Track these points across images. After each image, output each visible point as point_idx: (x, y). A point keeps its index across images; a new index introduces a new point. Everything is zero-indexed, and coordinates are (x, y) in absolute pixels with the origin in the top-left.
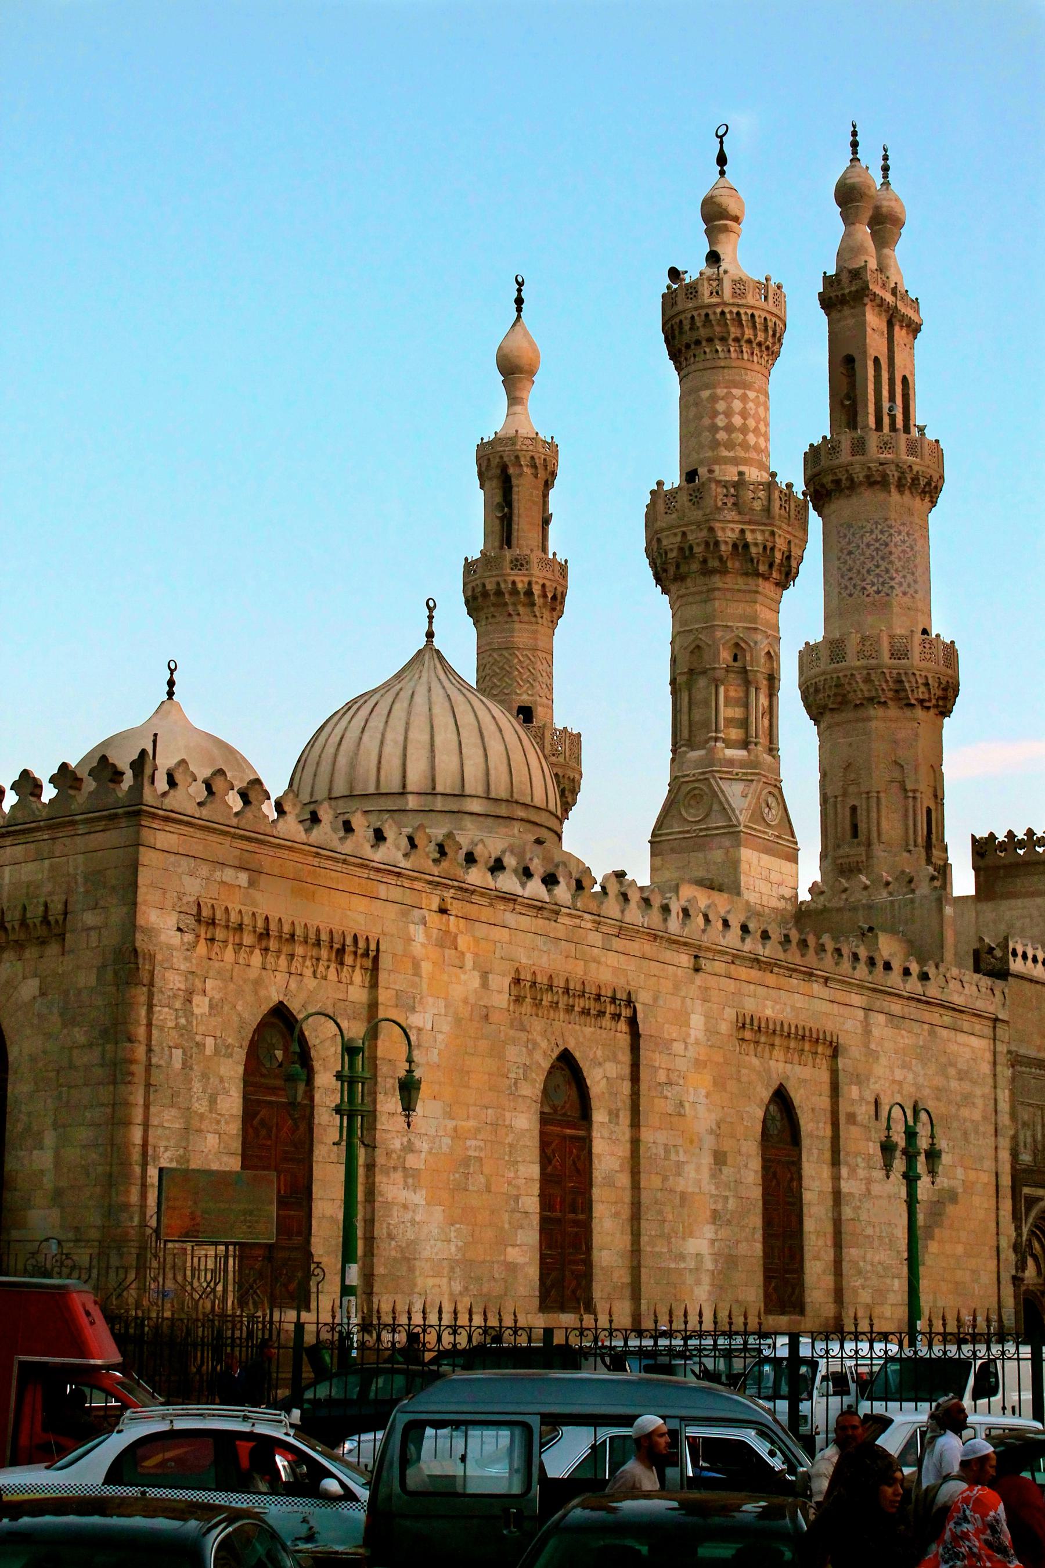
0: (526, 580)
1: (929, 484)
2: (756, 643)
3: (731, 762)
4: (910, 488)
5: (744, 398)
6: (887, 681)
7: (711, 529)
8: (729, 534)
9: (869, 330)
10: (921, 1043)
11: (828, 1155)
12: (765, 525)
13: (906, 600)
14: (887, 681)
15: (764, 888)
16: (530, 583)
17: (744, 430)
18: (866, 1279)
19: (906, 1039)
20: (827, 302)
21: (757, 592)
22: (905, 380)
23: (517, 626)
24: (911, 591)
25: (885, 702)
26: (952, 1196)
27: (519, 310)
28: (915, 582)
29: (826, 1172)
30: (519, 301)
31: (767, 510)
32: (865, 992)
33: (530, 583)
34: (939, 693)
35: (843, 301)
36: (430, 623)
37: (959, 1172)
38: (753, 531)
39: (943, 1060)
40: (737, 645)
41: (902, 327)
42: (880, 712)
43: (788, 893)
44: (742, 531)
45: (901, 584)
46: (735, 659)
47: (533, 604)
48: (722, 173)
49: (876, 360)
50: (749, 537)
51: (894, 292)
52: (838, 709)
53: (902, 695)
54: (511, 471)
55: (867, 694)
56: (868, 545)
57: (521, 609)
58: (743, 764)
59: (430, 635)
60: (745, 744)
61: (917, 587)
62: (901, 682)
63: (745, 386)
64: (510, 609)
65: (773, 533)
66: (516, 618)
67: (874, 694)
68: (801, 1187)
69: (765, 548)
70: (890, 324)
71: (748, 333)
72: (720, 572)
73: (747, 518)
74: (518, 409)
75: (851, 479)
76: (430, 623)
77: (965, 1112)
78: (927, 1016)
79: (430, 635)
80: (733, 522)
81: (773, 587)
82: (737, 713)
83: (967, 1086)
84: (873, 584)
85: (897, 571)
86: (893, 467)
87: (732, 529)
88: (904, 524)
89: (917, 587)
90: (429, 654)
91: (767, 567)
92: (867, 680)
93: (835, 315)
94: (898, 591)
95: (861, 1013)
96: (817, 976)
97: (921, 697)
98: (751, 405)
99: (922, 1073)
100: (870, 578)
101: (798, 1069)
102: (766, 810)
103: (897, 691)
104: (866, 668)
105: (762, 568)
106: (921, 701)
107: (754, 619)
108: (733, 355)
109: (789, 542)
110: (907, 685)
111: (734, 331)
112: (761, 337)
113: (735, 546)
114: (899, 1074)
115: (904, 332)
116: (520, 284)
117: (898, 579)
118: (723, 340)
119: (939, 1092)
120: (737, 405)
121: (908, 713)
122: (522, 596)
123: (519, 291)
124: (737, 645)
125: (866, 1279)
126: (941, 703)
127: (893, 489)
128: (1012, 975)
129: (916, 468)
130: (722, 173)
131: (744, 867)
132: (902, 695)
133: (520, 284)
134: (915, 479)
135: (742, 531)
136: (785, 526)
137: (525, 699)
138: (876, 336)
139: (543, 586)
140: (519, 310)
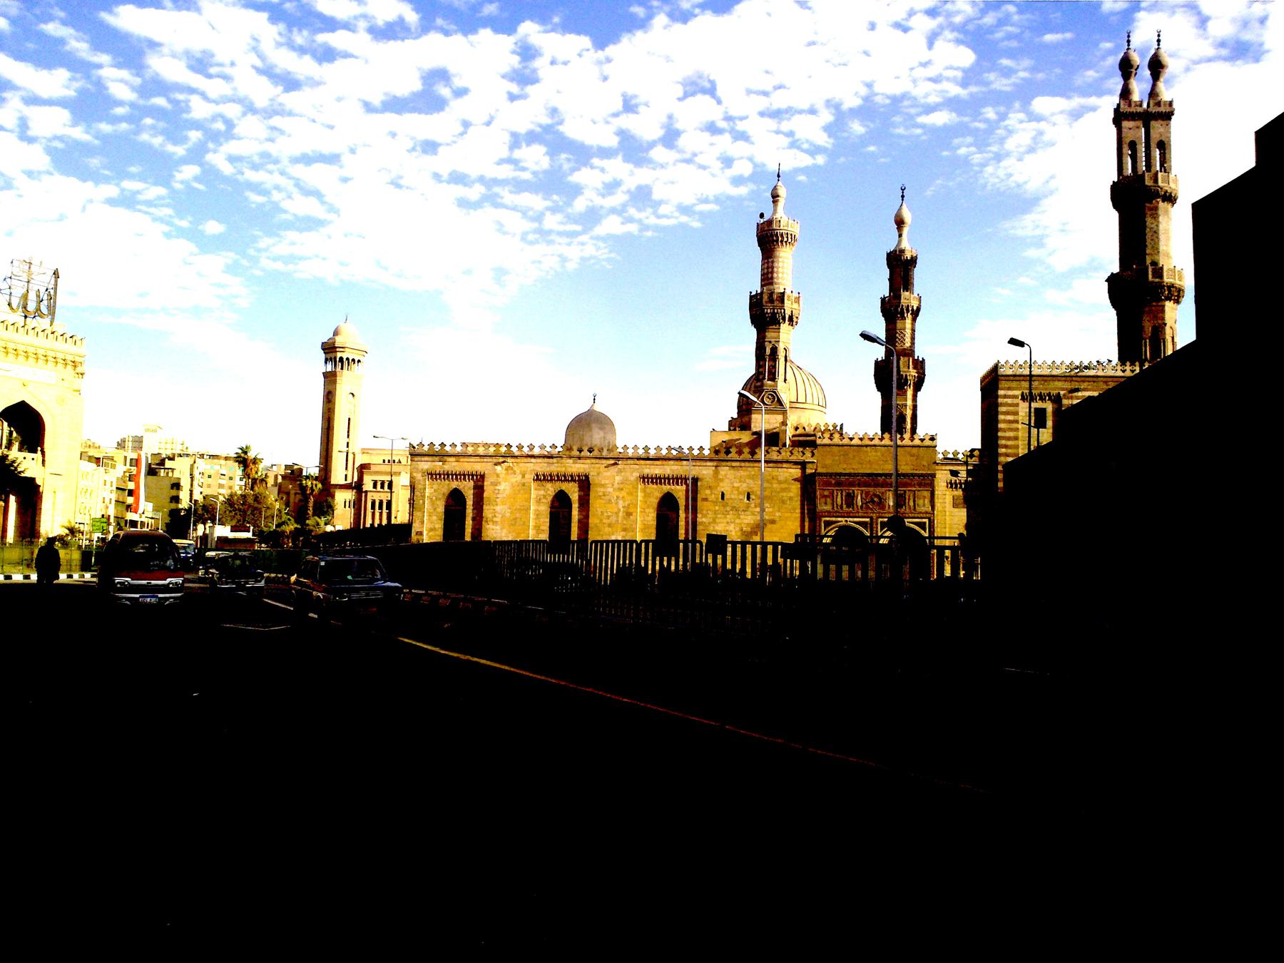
19: (742, 473)
26: (773, 522)
83: (783, 486)
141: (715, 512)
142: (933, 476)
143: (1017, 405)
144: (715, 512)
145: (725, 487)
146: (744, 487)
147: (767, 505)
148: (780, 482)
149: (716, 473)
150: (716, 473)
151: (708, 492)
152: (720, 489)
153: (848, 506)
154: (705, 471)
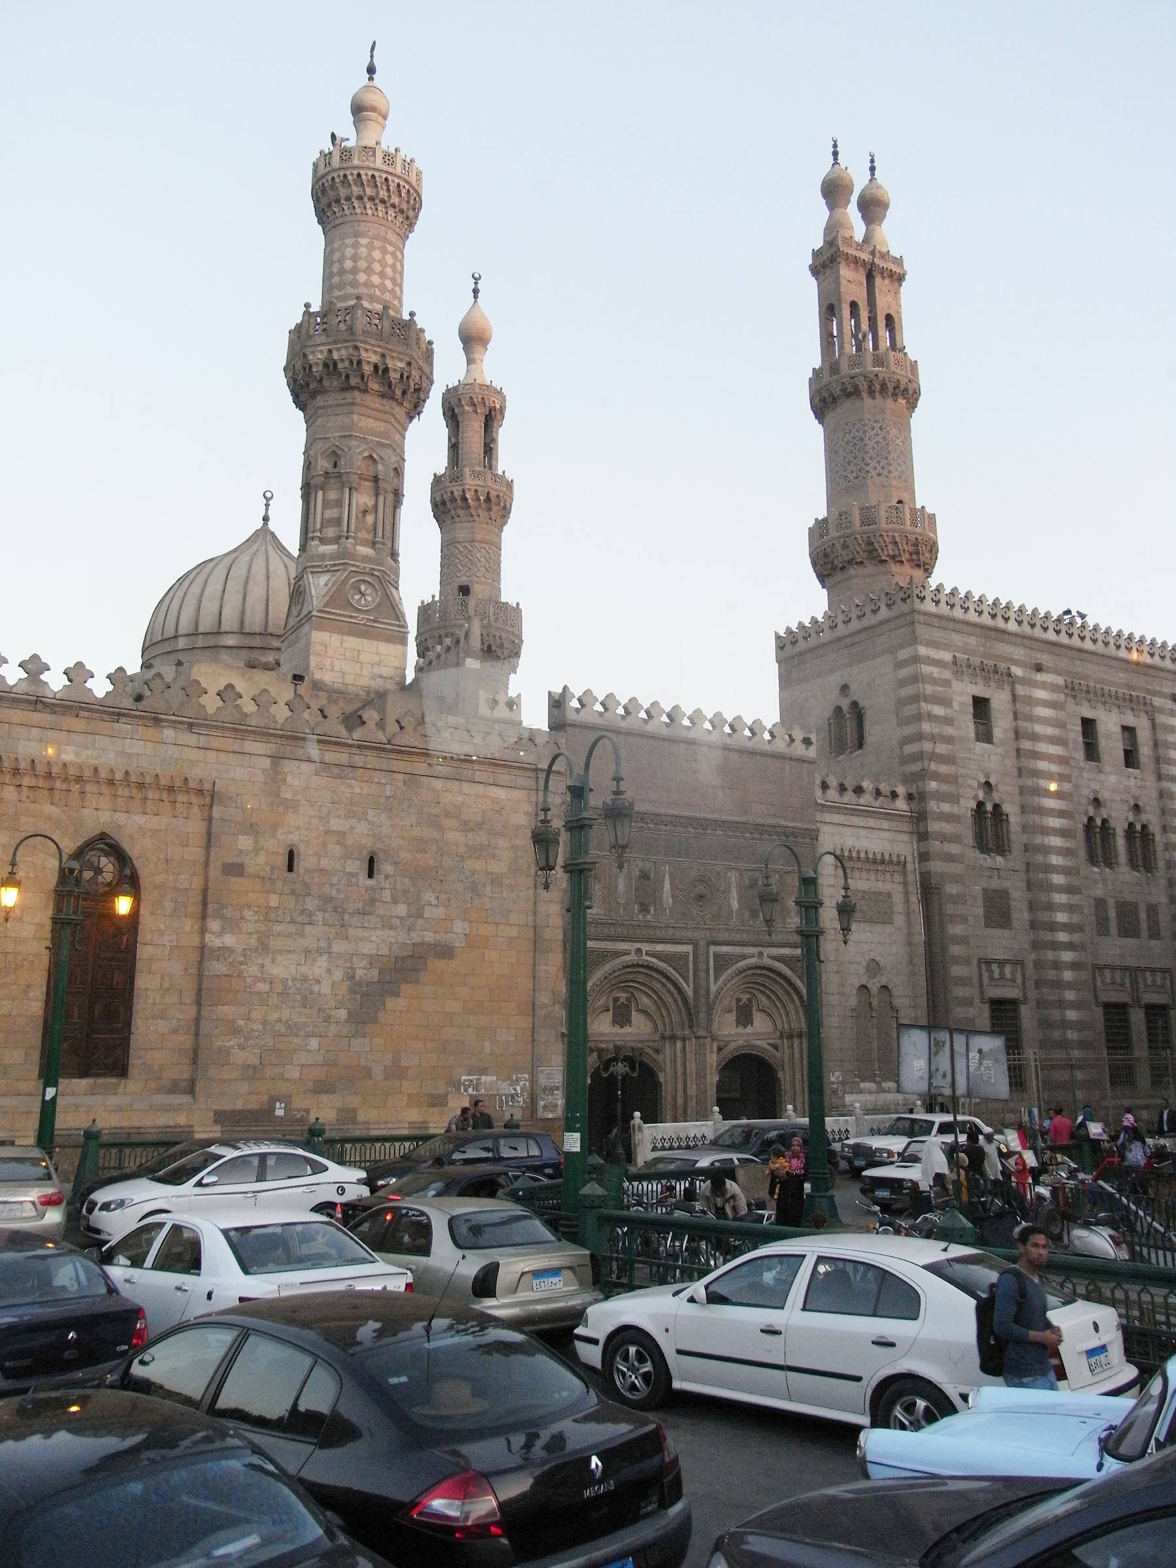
0: (460, 488)
1: (897, 387)
2: (350, 449)
3: (323, 557)
4: (881, 392)
5: (356, 245)
6: (860, 545)
7: (305, 356)
8: (320, 356)
9: (843, 282)
10: (388, 793)
11: (194, 908)
12: (347, 341)
13: (878, 480)
14: (860, 545)
15: (348, 668)
16: (464, 491)
17: (355, 271)
18: (247, 1038)
19: (356, 787)
20: (816, 270)
21: (353, 404)
22: (889, 319)
23: (459, 525)
24: (885, 472)
25: (861, 563)
26: (445, 951)
27: (476, 297)
28: (889, 464)
29: (189, 925)
30: (476, 292)
31: (351, 329)
32: (272, 739)
33: (464, 491)
34: (912, 549)
35: (824, 266)
36: (267, 510)
37: (460, 927)
38: (338, 349)
39: (435, 810)
40: (334, 452)
41: (883, 278)
42: (860, 570)
43: (387, 671)
44: (330, 351)
45: (875, 468)
46: (335, 465)
47: (469, 507)
48: (371, 79)
49: (854, 305)
50: (336, 356)
51: (873, 253)
52: (828, 575)
53: (875, 554)
54: (456, 411)
55: (846, 558)
56: (847, 443)
57: (461, 513)
58: (332, 557)
59: (266, 519)
60: (336, 540)
61: (891, 468)
62: (872, 543)
63: (357, 235)
64: (452, 512)
65: (356, 348)
66: (456, 519)
67: (851, 556)
68: (136, 942)
69: (351, 362)
70: (870, 277)
71: (356, 190)
72: (321, 392)
73: (332, 339)
74: (473, 366)
75: (831, 395)
76: (267, 510)
77: (479, 865)
78: (401, 765)
79: (266, 519)
80: (323, 344)
81: (378, 400)
82: (331, 513)
84: (852, 472)
85: (871, 458)
86: (862, 379)
87: (322, 352)
88: (876, 421)
89: (891, 468)
90: (264, 535)
91: (358, 380)
92: (845, 546)
93: (821, 277)
94: (874, 473)
95: (267, 763)
96: (165, 721)
97: (891, 552)
98: (363, 249)
99: (387, 823)
100: (849, 468)
101: (139, 820)
102: (357, 597)
103: (870, 552)
104: (843, 537)
105: (398, 393)
106: (893, 557)
107: (351, 427)
108: (358, 211)
109: (383, 356)
110: (876, 545)
111: (343, 192)
112: (369, 191)
113: (326, 365)
114: (336, 824)
115: (887, 281)
116: (477, 280)
117: (873, 464)
118: (338, 201)
119: (420, 844)
120: (349, 251)
121: (882, 568)
122: (459, 501)
123: (476, 283)
124: (334, 452)
125: (247, 1038)
126: (914, 557)
127: (865, 395)
128: (572, 725)
129: (881, 376)
130: (371, 79)
131: (316, 648)
132: (875, 554)
133: (477, 280)
134: (883, 386)
135: (330, 351)
136: (373, 342)
137: (464, 580)
138: (852, 286)
139: (476, 491)
140: (476, 297)
141: (268, 915)
142: (814, 836)
143: (946, 683)
144: (268, 915)
145: (296, 828)
146: (361, 834)
147: (429, 896)
148: (466, 827)
149: (275, 778)
150: (275, 778)
151: (245, 842)
152: (287, 836)
153: (644, 909)
154: (240, 771)
